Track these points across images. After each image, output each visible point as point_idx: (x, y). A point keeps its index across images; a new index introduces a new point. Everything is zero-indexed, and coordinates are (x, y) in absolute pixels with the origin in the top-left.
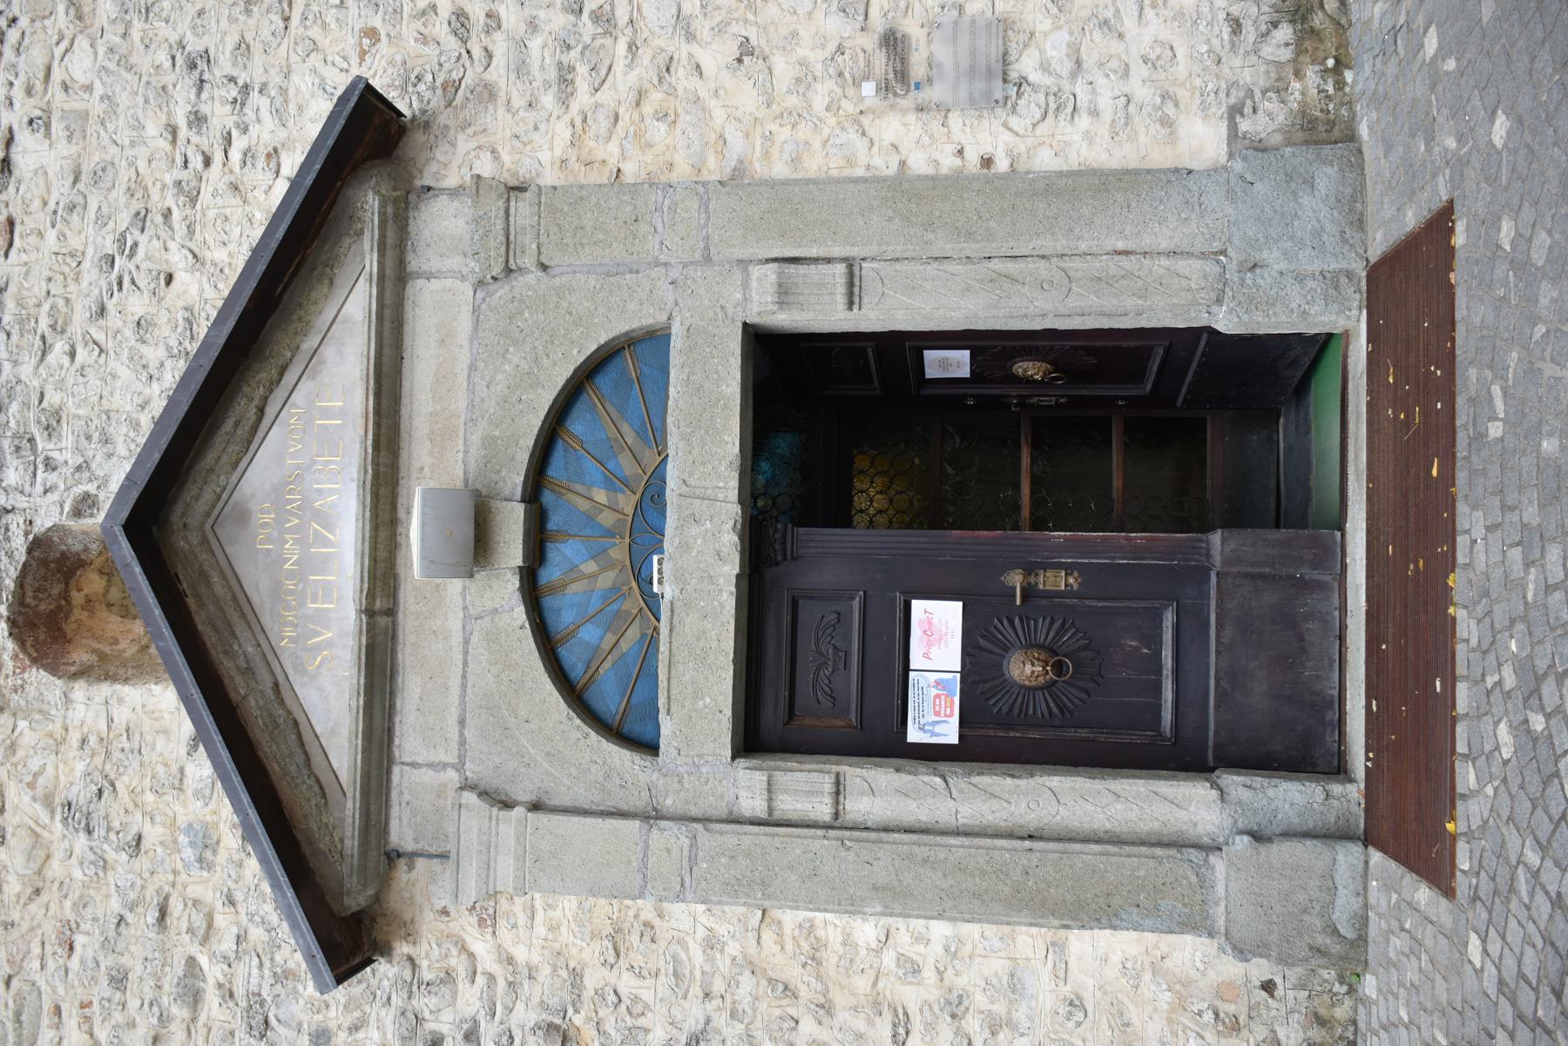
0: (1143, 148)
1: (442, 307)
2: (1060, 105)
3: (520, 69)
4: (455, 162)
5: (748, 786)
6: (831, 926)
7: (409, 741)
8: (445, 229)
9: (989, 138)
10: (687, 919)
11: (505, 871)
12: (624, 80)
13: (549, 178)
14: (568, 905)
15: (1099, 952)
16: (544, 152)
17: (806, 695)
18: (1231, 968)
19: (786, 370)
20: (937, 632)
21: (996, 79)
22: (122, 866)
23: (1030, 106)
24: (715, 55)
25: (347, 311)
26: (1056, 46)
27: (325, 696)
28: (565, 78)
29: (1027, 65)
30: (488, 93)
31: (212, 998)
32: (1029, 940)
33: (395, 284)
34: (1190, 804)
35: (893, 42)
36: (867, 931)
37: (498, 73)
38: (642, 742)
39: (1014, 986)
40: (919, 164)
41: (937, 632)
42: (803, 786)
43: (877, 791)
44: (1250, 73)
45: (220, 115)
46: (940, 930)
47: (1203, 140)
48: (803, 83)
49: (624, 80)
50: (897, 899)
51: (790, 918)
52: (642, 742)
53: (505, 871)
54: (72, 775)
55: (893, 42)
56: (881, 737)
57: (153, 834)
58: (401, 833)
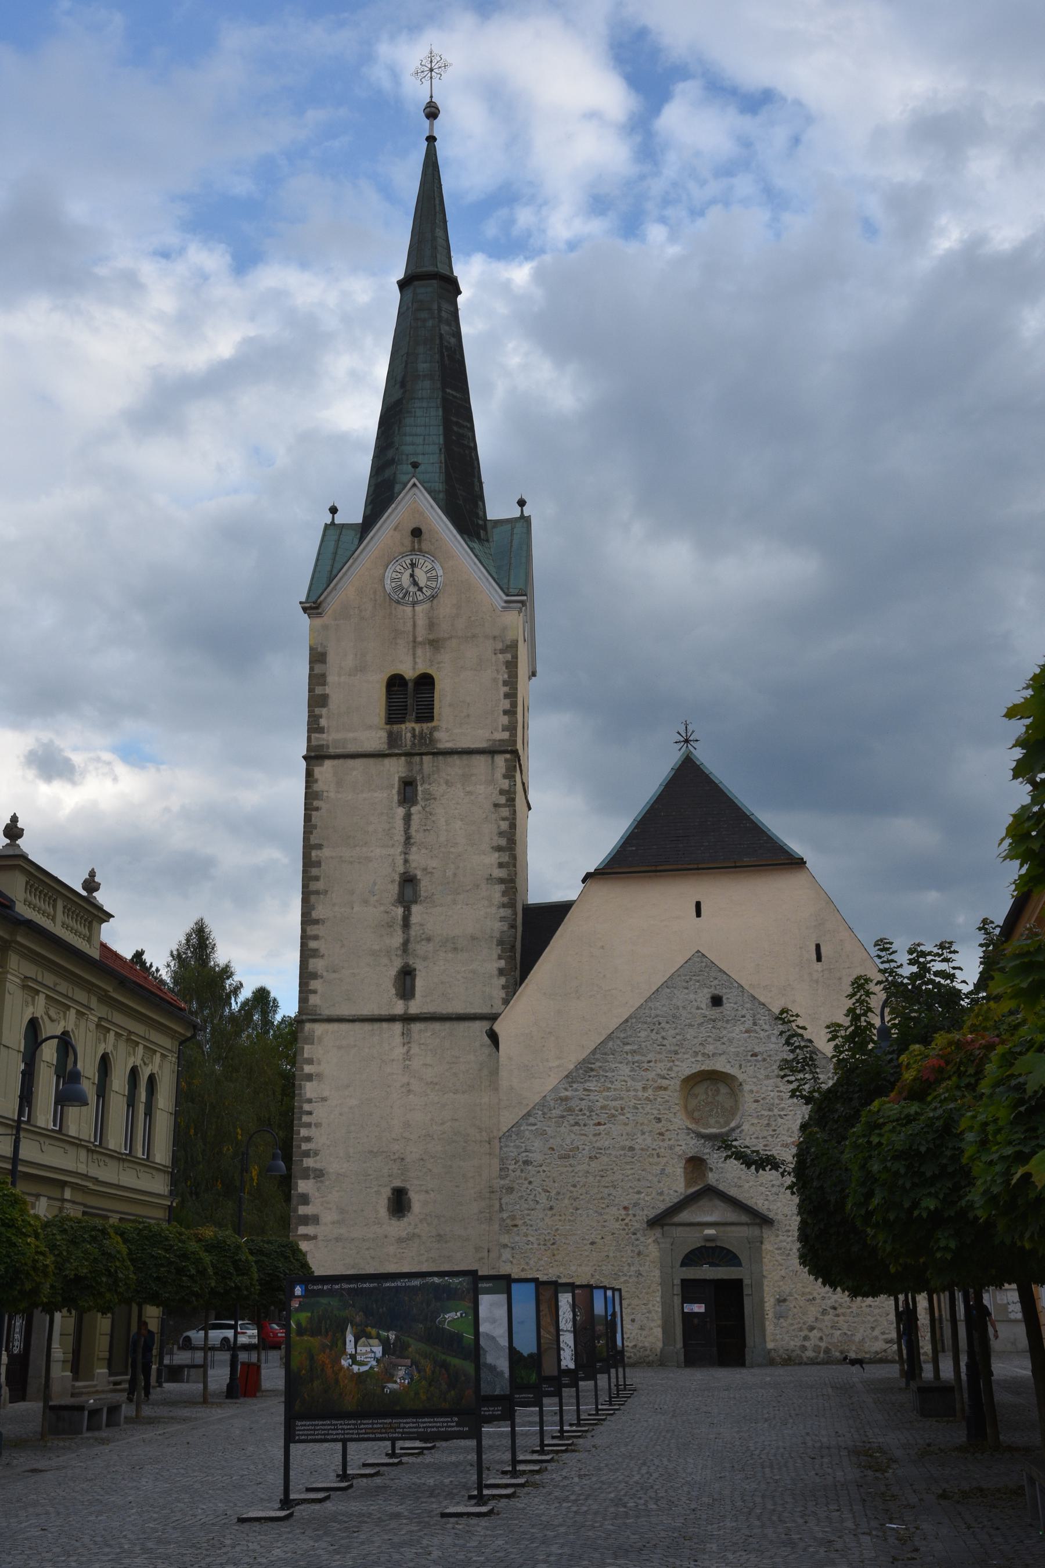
0: (769, 1337)
1: (744, 1232)
2: (776, 1325)
3: (781, 1241)
4: (767, 1233)
5: (677, 1282)
6: (659, 1294)
7: (680, 1229)
8: (755, 1231)
9: (770, 1315)
10: (657, 1273)
11: (663, 1246)
12: (779, 1258)
13: (764, 1247)
14: (658, 1254)
15: (658, 1332)
16: (767, 1246)
17: (690, 1290)
18: (659, 1350)
19: (736, 1286)
20: (699, 1308)
21: (779, 1316)
22: (656, 1180)
23: (776, 1321)
24: (783, 1273)
25: (744, 1218)
26: (785, 1324)
27: (685, 1216)
28: (780, 1249)
29: (782, 1320)
30: (777, 1236)
31: (637, 1196)
32: (659, 1322)
33: (747, 1224)
34: (679, 1344)
35: (785, 1300)
36: (658, 1299)
37: (781, 1238)
38: (683, 1264)
39: (653, 1320)
40: (766, 1305)
41: (699, 1308)
42: (677, 1290)
43: (677, 1300)
44: (781, 1351)
45: (774, 1190)
46: (660, 1310)
47: (770, 1345)
48: (779, 1287)
49: (779, 1258)
50: (664, 1304)
51: (659, 1288)
52: (683, 1264)
53: (663, 1246)
54: (669, 1170)
55: (785, 1300)
56: (686, 1300)
57: (661, 1185)
58: (666, 1228)
